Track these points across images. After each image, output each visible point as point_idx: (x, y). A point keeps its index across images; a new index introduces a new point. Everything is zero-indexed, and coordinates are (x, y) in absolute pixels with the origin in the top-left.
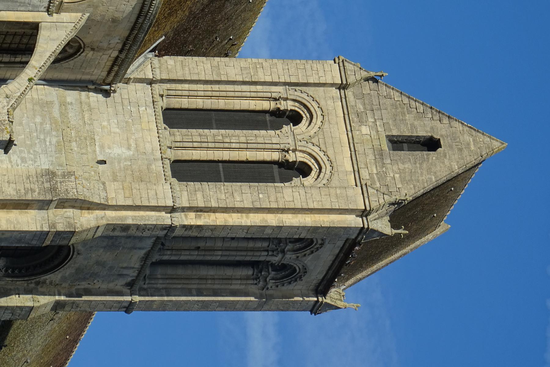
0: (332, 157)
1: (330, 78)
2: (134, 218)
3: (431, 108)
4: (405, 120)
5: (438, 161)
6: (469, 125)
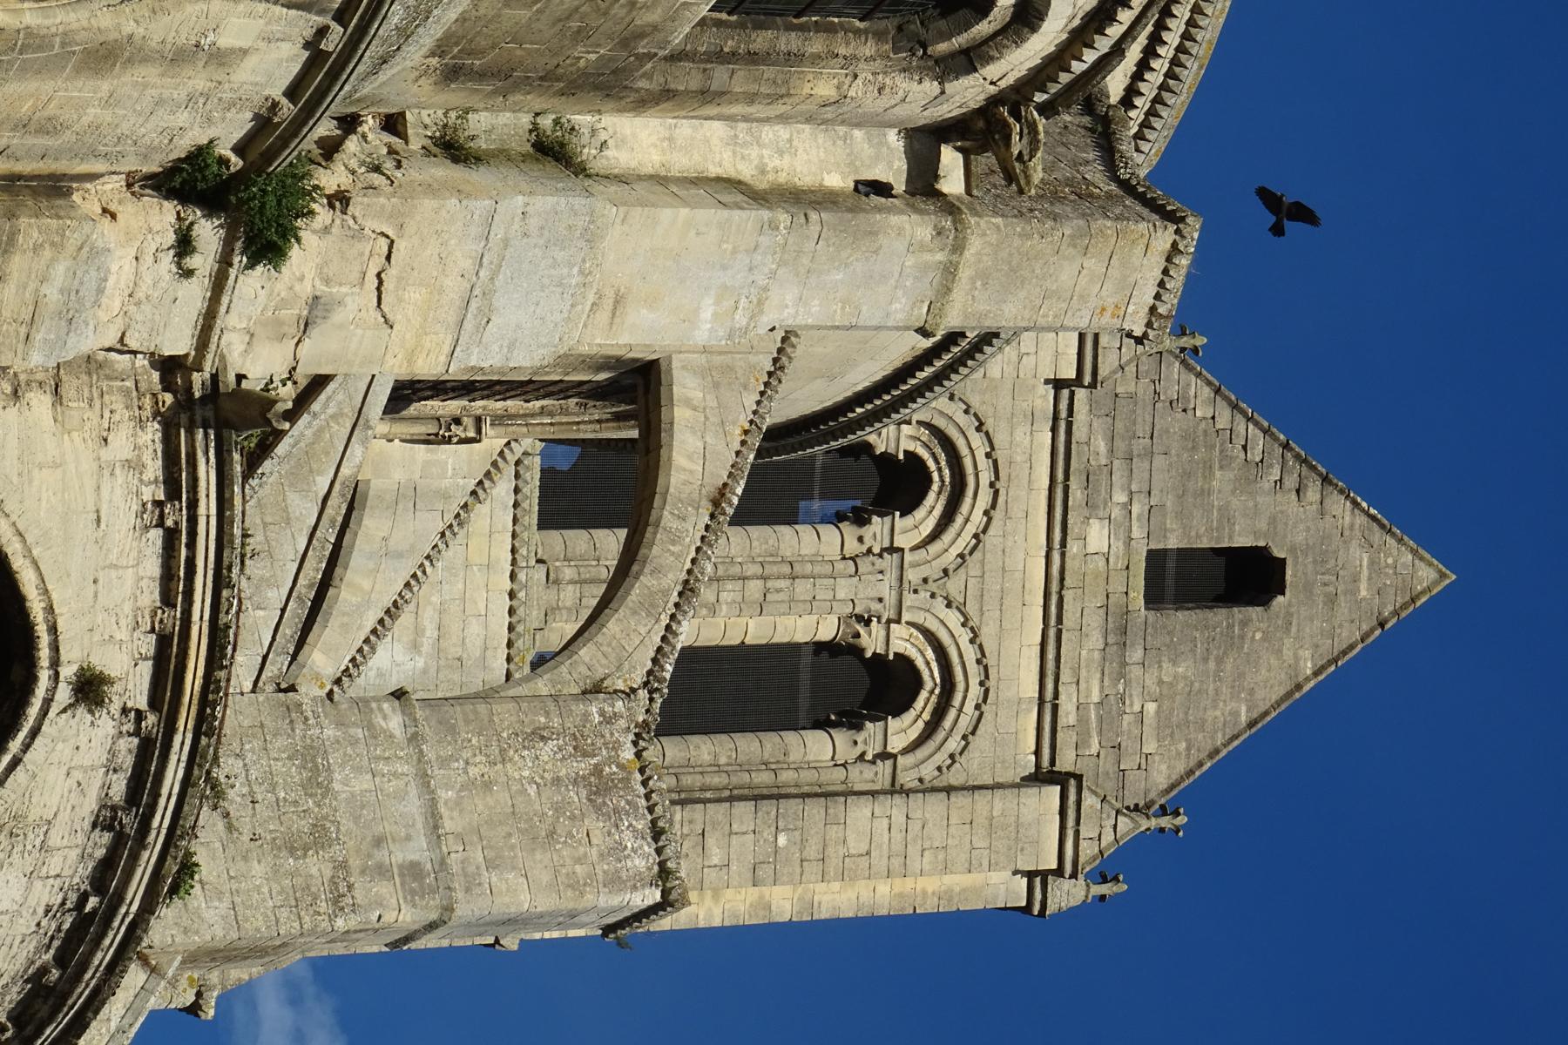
0: (990, 660)
1: (1049, 358)
3: (1286, 446)
4: (1209, 494)
5: (1266, 645)
6: (1373, 511)
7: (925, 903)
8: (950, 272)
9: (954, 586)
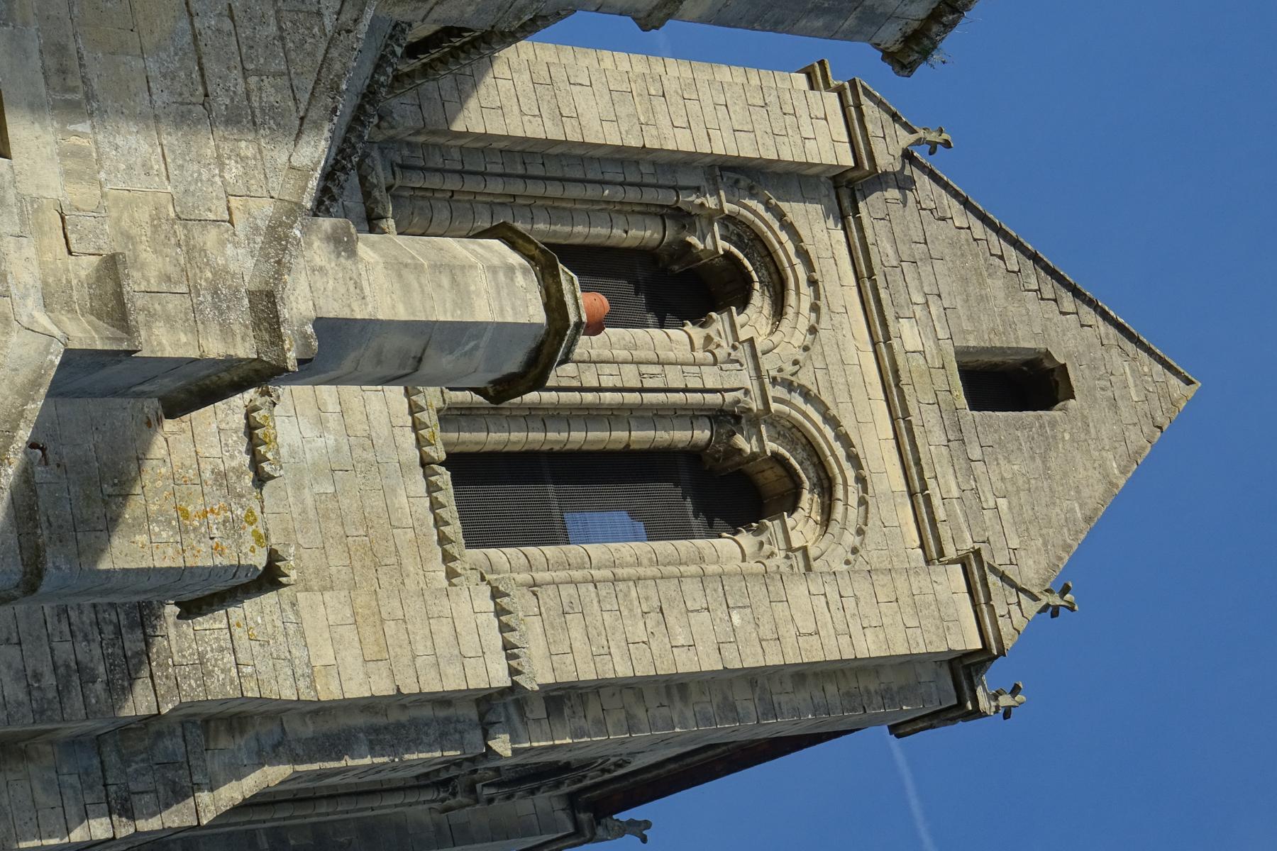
7: (872, 702)
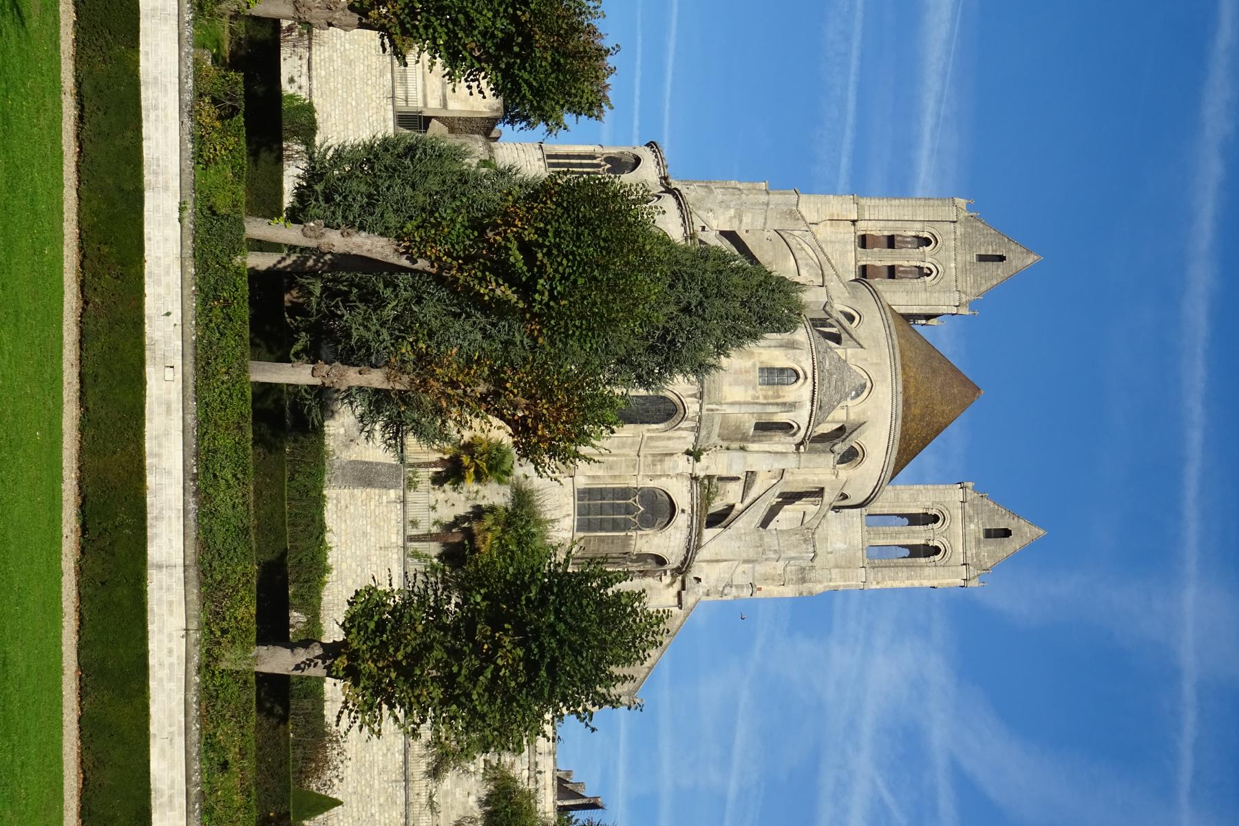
2: (844, 586)
8: (800, 461)
9: (945, 535)
